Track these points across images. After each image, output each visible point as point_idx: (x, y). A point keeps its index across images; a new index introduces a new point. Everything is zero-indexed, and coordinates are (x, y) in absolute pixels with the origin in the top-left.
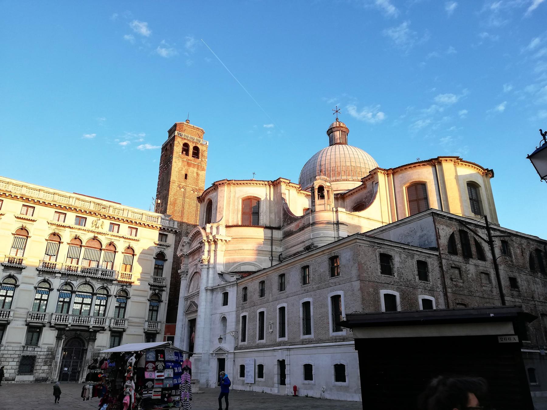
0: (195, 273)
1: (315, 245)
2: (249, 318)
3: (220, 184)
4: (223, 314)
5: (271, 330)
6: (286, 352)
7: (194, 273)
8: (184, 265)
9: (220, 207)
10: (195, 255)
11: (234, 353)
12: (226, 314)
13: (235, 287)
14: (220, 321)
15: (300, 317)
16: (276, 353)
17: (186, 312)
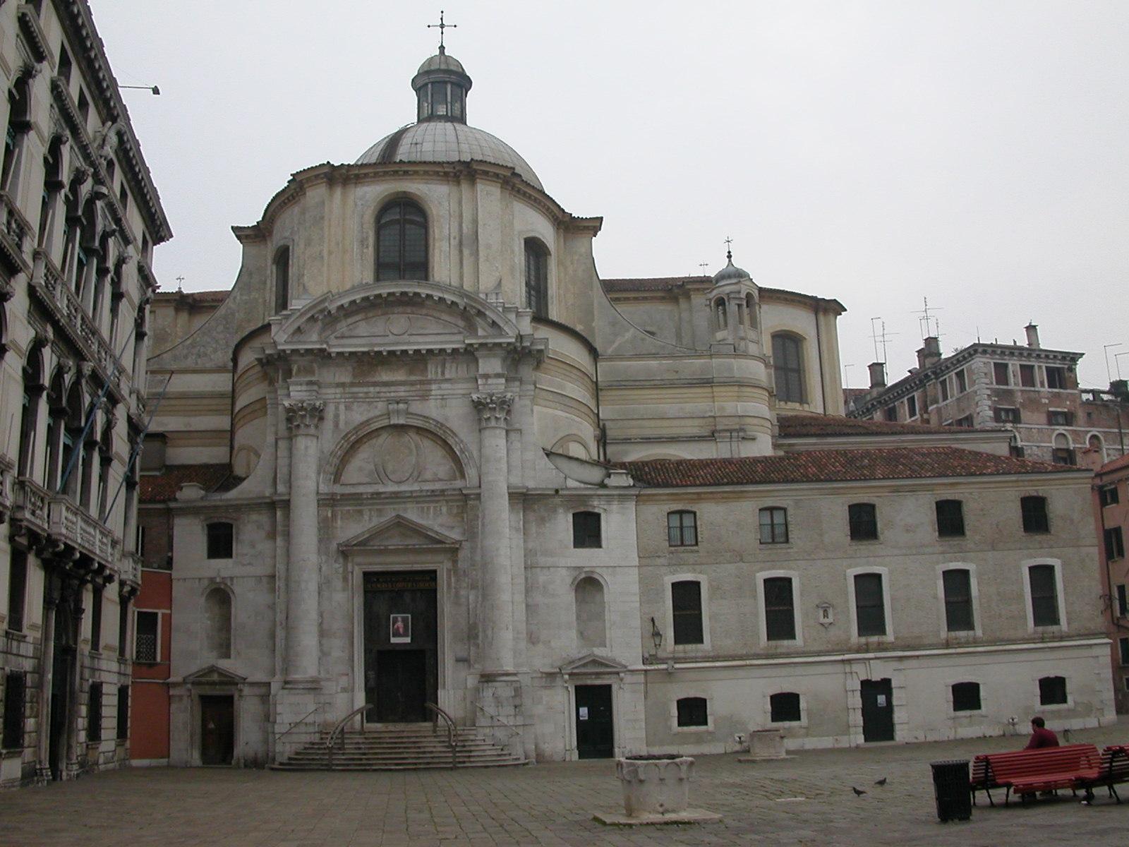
0: (395, 427)
1: (748, 433)
2: (714, 589)
3: (486, 173)
4: (584, 570)
5: (830, 620)
6: (896, 665)
7: (385, 422)
8: (315, 388)
9: (489, 247)
10: (377, 365)
11: (646, 671)
12: (598, 570)
13: (631, 506)
14: (574, 587)
15: (935, 597)
16: (856, 667)
17: (354, 545)
